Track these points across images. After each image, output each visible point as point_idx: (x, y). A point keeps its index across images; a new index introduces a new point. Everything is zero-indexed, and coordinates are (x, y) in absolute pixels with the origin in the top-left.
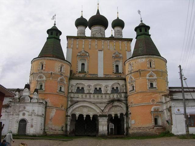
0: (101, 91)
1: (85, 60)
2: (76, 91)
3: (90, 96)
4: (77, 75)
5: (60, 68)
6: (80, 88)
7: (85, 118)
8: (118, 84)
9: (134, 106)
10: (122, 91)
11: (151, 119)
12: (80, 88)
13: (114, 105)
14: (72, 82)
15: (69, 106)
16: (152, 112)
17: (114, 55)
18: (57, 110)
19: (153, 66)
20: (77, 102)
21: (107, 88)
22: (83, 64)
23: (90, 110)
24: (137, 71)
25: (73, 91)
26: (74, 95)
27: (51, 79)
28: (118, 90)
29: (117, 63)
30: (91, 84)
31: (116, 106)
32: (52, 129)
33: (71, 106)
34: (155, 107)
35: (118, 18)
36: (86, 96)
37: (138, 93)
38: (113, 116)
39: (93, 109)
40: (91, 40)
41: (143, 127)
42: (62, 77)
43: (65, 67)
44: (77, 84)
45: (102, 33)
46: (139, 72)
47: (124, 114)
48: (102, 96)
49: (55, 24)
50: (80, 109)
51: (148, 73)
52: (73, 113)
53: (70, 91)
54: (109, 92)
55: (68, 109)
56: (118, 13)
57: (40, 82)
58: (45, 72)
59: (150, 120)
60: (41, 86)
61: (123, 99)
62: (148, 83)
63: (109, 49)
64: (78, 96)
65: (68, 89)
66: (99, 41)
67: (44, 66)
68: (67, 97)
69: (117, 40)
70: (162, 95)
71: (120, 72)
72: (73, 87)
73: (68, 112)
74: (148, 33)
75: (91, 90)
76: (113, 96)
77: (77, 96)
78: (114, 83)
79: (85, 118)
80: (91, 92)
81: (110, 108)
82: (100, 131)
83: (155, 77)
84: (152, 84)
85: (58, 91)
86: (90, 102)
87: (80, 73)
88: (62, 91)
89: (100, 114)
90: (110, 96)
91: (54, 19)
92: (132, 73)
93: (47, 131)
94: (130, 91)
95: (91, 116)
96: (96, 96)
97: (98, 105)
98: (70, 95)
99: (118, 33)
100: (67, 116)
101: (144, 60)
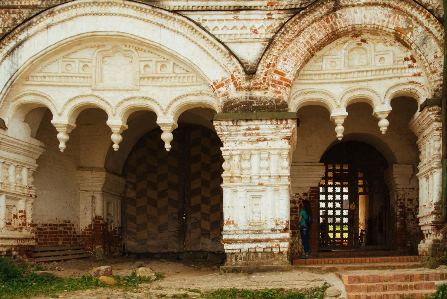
23: (154, 69)
50: (76, 68)
89: (234, 94)
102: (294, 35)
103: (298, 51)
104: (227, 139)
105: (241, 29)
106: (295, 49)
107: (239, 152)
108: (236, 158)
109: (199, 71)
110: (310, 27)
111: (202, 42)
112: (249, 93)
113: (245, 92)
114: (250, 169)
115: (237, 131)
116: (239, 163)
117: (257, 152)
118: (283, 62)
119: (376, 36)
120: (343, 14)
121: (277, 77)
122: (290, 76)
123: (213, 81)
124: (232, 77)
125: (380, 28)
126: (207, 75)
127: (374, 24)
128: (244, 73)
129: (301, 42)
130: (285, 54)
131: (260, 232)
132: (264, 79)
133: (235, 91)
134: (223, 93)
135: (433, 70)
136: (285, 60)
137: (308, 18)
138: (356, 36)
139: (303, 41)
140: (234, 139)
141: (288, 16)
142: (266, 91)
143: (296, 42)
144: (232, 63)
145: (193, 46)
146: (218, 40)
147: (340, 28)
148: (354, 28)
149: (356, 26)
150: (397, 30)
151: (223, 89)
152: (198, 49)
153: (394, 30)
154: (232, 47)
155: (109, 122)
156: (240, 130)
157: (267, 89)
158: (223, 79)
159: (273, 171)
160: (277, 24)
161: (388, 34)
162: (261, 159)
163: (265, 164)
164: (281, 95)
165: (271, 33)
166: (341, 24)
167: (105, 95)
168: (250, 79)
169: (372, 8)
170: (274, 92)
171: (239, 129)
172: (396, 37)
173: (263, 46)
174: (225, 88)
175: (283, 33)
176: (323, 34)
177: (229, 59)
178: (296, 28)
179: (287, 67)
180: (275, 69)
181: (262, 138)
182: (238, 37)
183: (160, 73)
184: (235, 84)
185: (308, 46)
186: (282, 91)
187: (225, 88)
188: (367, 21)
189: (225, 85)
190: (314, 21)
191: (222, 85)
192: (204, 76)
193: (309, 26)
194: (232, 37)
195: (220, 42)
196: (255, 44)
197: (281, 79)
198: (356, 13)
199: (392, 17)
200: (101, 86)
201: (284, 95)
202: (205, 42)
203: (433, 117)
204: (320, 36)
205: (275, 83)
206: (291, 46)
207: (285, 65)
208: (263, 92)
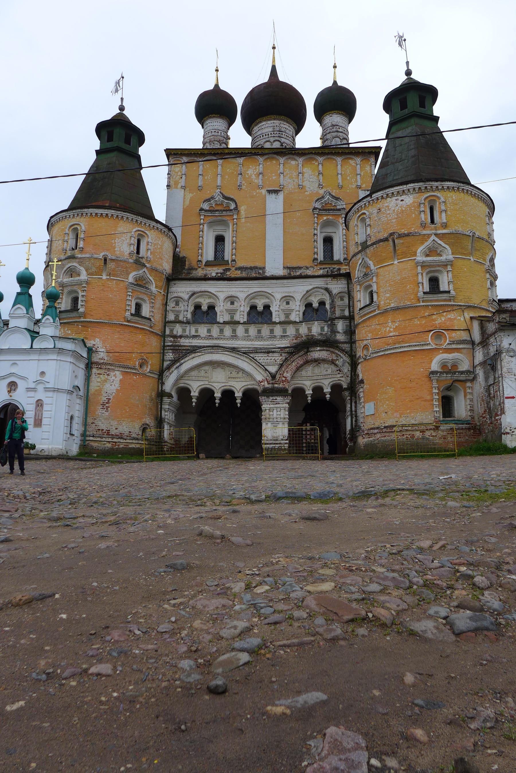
0: (271, 313)
1: (224, 223)
2: (189, 316)
3: (234, 331)
4: (200, 273)
5: (134, 241)
6: (204, 308)
7: (220, 399)
8: (327, 289)
10: (338, 313)
11: (429, 398)
12: (204, 308)
13: (309, 358)
14: (179, 289)
15: (166, 364)
16: (433, 373)
17: (318, 205)
18: (124, 373)
19: (440, 218)
20: (194, 350)
21: (288, 303)
22: (220, 240)
23: (234, 374)
24: (386, 240)
25: (181, 318)
26: (184, 330)
27: (104, 277)
28: (326, 311)
29: (329, 231)
30: (242, 296)
31: (317, 361)
32: (108, 434)
33: (174, 362)
34: (446, 356)
35: (335, 83)
36: (222, 331)
37: (386, 311)
38: (309, 392)
39: (243, 371)
40: (243, 158)
41: (403, 426)
42: (141, 272)
43: (150, 240)
44: (194, 294)
45: (286, 141)
46: (391, 242)
47: (345, 386)
48: (272, 331)
49: (122, 108)
50: (202, 373)
51: (423, 243)
52: (182, 385)
53: (171, 317)
54: (295, 317)
55: (166, 373)
56: (335, 67)
57: (69, 288)
58: (83, 256)
59: (426, 401)
60: (75, 300)
61: (340, 337)
62: (420, 276)
63: (301, 187)
64: (197, 331)
65: (166, 311)
67: (81, 235)
68: (163, 336)
69: (328, 154)
70: (472, 318)
71: (336, 257)
72: (181, 304)
73: (163, 384)
74: (429, 113)
75: (238, 313)
76: (310, 329)
77: (193, 333)
78: (310, 287)
79: (217, 401)
80: (237, 317)
81: (299, 369)
82: (264, 440)
83: (448, 255)
84: (434, 282)
85: (128, 314)
86: (234, 350)
87: (208, 264)
88: (143, 314)
89: (267, 385)
90: (297, 330)
91: (120, 92)
92: (368, 247)
93: (91, 438)
94: (360, 309)
95: (238, 394)
96: (253, 330)
97: (261, 358)
98: (172, 331)
99: (334, 134)
100: (161, 395)
101: (409, 199)
108: (268, 411)
111: (254, 365)
114: (273, 415)
121: (284, 379)
122: (289, 379)
131: (277, 440)
137: (297, 356)
138: (316, 361)
145: (251, 366)
148: (315, 359)
150: (332, 360)
151: (262, 384)
154: (266, 367)
155: (215, 395)
159: (282, 416)
163: (279, 413)
167: (215, 385)
178: (292, 359)
183: (236, 376)
188: (320, 357)
191: (262, 382)
200: (212, 380)
204: (301, 362)
205: (283, 381)
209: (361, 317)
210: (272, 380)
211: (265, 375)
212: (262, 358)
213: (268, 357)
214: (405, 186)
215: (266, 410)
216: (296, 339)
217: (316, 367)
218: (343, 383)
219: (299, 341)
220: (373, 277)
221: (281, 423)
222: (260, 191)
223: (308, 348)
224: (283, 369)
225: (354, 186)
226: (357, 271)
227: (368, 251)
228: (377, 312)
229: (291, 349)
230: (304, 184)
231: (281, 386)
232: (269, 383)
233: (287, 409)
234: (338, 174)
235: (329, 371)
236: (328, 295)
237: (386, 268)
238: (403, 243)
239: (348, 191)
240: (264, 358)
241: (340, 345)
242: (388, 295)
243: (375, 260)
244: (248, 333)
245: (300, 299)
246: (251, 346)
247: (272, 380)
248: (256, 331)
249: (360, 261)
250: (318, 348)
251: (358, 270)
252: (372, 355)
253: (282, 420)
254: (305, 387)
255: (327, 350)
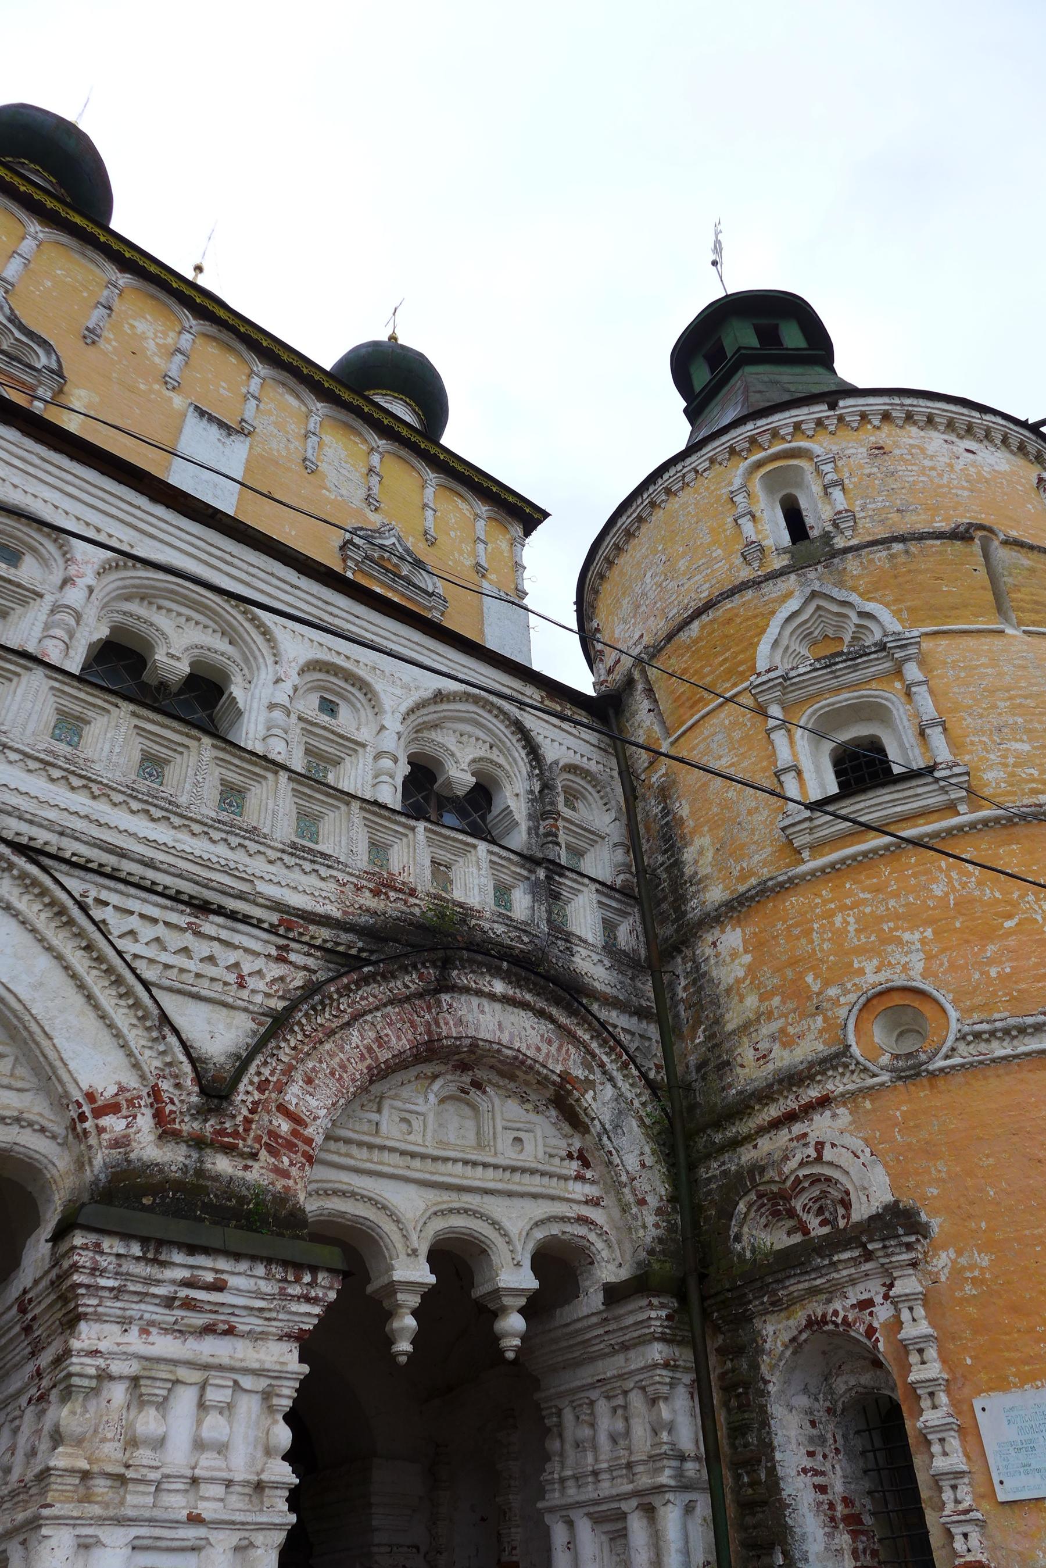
9: (1000, 1049)
13: (449, 1028)
21: (329, 707)
66: (212, 350)
102: (341, 1022)
103: (343, 1067)
104: (100, 1309)
105: (202, 960)
106: (337, 1059)
107: (132, 1368)
108: (118, 1392)
109: (45, 1043)
110: (379, 1014)
111: (79, 961)
112: (195, 1155)
113: (183, 1149)
114: (159, 1443)
115: (149, 1281)
116: (124, 1412)
117: (196, 1376)
118: (305, 1086)
119: (507, 1081)
120: (455, 1005)
121: (285, 1127)
123: (85, 1087)
124: (155, 1093)
125: (529, 1062)
126: (72, 1065)
127: (519, 1051)
128: (196, 1089)
129: (354, 1045)
130: (310, 1065)
132: (247, 1121)
133: (152, 1138)
134: (113, 1136)
135: (640, 1196)
136: (309, 1081)
138: (463, 1067)
139: (359, 1043)
140: (128, 1313)
141: (330, 970)
142: (250, 1163)
143: (340, 1042)
144: (162, 1048)
145: (44, 962)
146: (133, 970)
147: (446, 1037)
148: (474, 1044)
149: (481, 1043)
151: (115, 1124)
152: (58, 978)
153: (559, 1076)
156: (159, 1282)
157: (254, 1156)
158: (122, 1089)
160: (298, 979)
161: (543, 1082)
162: (202, 1406)
164: (291, 1183)
165: (279, 997)
166: (450, 1029)
168: (210, 1110)
169: (516, 1010)
170: (271, 1170)
171: (160, 1276)
172: (557, 1094)
173: (254, 1026)
174: (123, 1123)
175: (314, 1008)
176: (408, 1040)
177: (155, 1034)
179: (313, 1103)
180: (281, 1101)
181: (224, 1322)
182: (189, 978)
184: (159, 1117)
185: (369, 1061)
186: (294, 1171)
187: (123, 1123)
188: (505, 1039)
189: (124, 1112)
190: (391, 1002)
191: (113, 1108)
192: (58, 1064)
193: (377, 1009)
194: (173, 973)
195: (138, 977)
196: (233, 1013)
197: (295, 1133)
198: (483, 1012)
199: (556, 1045)
201: (299, 1186)
202: (88, 963)
203: (656, 1327)
204: (401, 1042)
205: (275, 1144)
206: (327, 1046)
207: (308, 1098)
208: (240, 1163)
209: (817, 848)
210: (202, 1113)
211: (151, 1062)
212: (147, 932)
213: (188, 940)
214: (977, 415)
215: (104, 1376)
216: (376, 893)
217: (450, 1107)
218: (599, 1245)
219: (390, 906)
220: (908, 659)
221: (224, 1540)
222: (171, 394)
223: (445, 965)
224: (285, 1054)
225: (469, 562)
226: (764, 648)
227: (852, 565)
228: (965, 816)
229: (345, 937)
230: (323, 467)
231: (257, 1174)
232: (166, 1132)
233: (286, 1397)
234: (425, 506)
235: (532, 1153)
236: (520, 754)
237: (971, 642)
238: (1032, 570)
239: (450, 563)
240: (160, 930)
241: (595, 1007)
242: (1026, 747)
243: (896, 601)
244: (76, 747)
245: (403, 708)
246: (79, 825)
247: (202, 1113)
248: (137, 756)
249: (793, 605)
250: (499, 987)
251: (776, 643)
252: (962, 1047)
253: (237, 1506)
254: (388, 1227)
255: (541, 1014)
